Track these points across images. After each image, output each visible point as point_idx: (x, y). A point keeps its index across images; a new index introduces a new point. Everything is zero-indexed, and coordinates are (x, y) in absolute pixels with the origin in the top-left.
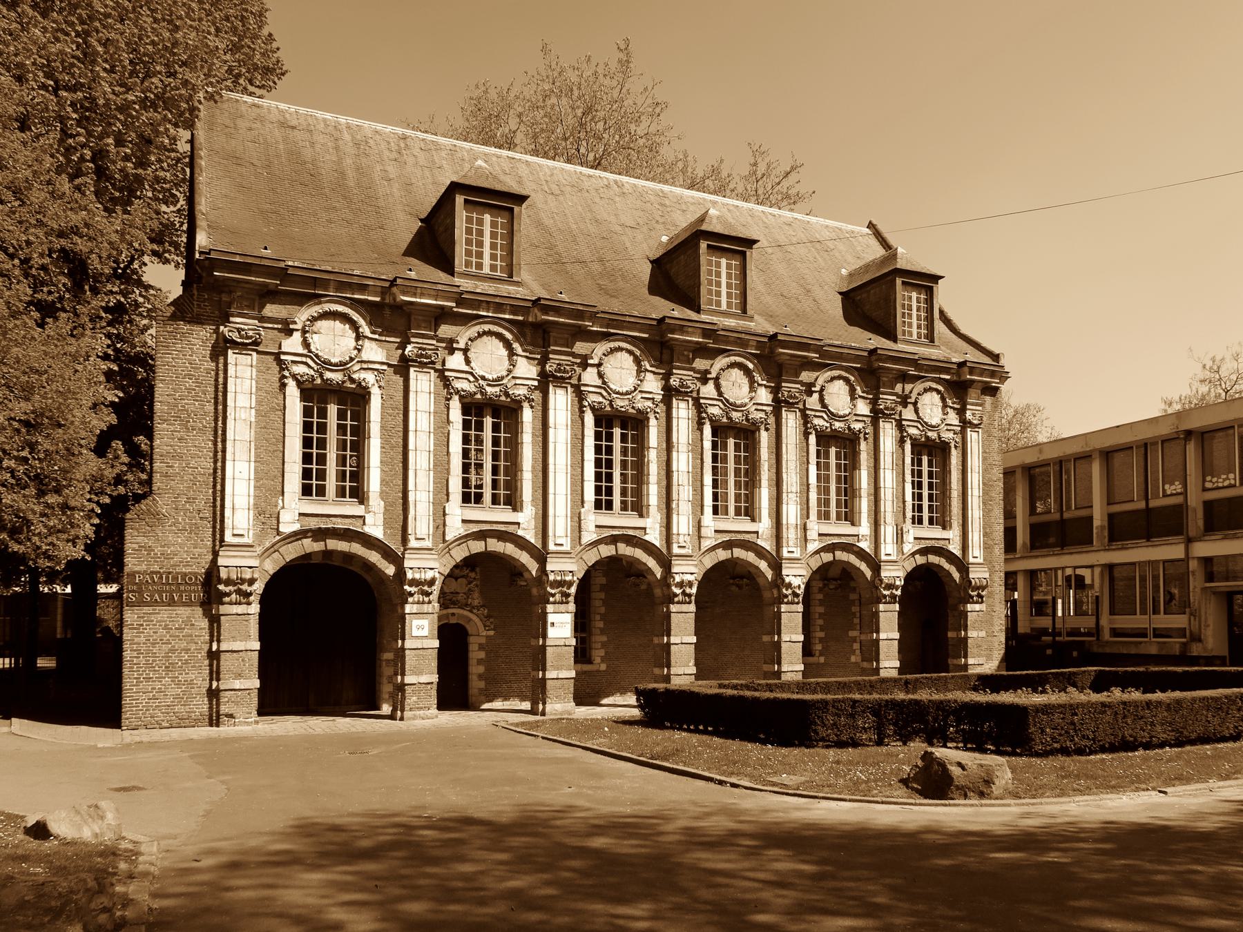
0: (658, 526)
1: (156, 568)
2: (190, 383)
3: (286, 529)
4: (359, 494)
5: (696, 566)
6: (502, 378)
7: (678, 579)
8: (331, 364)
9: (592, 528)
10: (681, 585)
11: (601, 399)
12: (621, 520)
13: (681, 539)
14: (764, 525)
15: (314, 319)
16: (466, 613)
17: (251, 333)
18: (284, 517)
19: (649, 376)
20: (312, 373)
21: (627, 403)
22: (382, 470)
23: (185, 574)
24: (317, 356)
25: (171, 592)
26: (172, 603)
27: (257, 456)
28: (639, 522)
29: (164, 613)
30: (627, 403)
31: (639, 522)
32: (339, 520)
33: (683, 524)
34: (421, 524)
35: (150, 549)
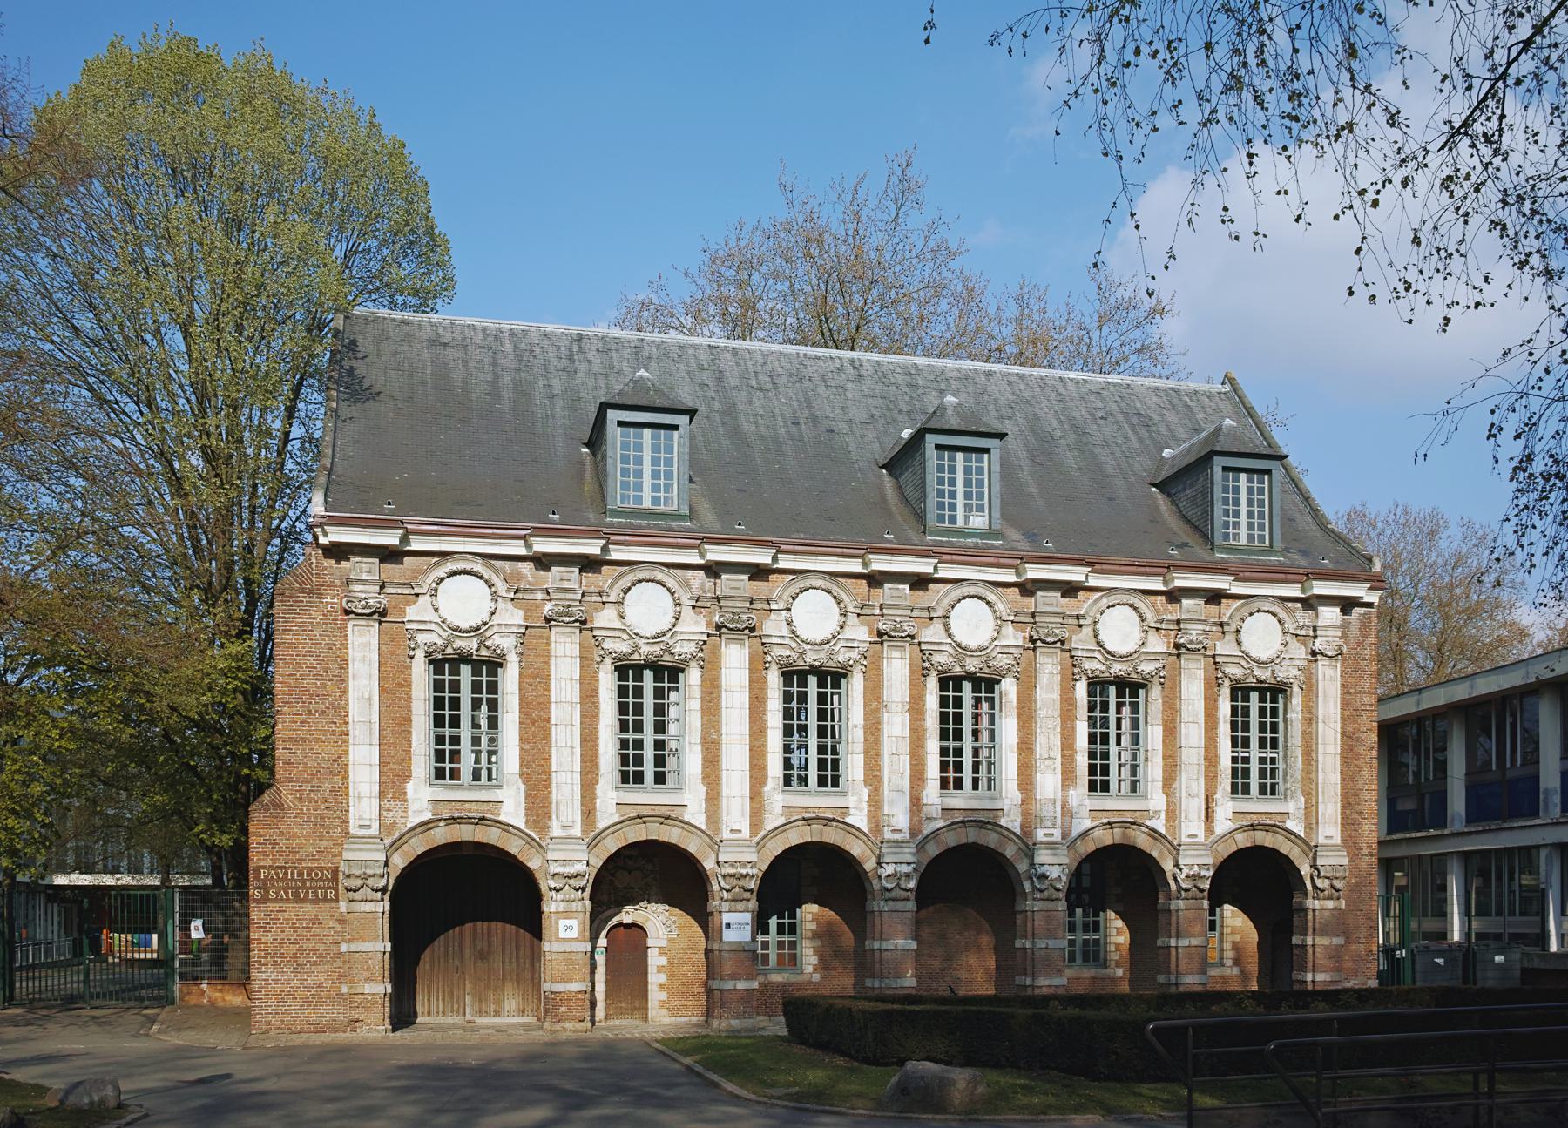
1: (281, 863)
7: (889, 869)
12: (816, 799)
23: (311, 869)
25: (297, 889)
26: (298, 899)
29: (292, 911)
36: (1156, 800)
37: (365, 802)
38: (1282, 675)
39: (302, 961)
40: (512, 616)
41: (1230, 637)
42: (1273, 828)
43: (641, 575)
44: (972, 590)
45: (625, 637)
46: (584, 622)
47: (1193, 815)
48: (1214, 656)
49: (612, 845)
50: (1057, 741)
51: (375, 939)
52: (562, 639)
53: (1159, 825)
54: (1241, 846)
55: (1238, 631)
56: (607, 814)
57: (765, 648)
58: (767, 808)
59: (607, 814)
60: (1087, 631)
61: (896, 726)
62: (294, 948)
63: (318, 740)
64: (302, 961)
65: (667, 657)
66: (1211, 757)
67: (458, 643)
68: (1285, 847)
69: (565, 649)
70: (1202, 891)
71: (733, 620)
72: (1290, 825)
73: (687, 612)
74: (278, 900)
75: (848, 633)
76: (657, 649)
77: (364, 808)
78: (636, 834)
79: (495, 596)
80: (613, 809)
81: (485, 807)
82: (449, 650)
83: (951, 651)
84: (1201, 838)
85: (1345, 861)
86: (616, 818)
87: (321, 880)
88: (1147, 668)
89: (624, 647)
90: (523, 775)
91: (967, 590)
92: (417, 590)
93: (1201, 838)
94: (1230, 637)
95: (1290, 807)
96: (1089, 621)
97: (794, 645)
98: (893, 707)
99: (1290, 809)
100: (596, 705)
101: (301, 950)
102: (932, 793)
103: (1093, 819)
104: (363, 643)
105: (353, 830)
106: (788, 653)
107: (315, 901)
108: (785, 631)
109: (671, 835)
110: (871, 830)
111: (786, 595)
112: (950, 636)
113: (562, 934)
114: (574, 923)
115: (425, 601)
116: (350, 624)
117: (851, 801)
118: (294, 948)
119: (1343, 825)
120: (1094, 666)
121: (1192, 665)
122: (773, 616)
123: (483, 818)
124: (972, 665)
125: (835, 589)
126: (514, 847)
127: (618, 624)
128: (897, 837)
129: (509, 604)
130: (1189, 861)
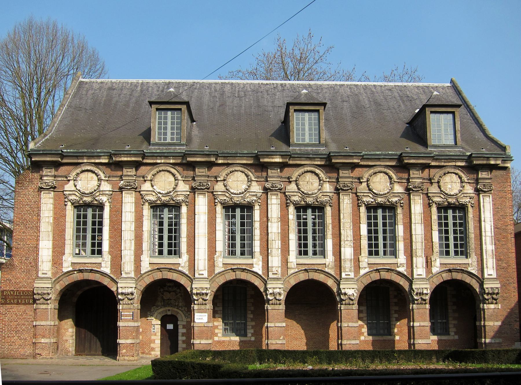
0: (261, 263)
1: (12, 288)
2: (28, 208)
3: (65, 270)
4: (100, 252)
5: (282, 284)
6: (170, 192)
7: (271, 291)
8: (85, 194)
9: (221, 265)
10: (273, 294)
11: (225, 198)
13: (274, 269)
14: (330, 258)
15: (78, 174)
16: (176, 310)
17: (50, 184)
18: (65, 265)
19: (254, 184)
20: (78, 198)
22: (110, 241)
24: (79, 191)
25: (18, 299)
26: (18, 303)
27: (54, 237)
28: (249, 261)
31: (249, 261)
32: (90, 265)
33: (275, 261)
35: (10, 281)
36: (402, 258)
37: (45, 264)
38: (463, 200)
39: (19, 328)
40: (106, 187)
41: (435, 185)
43: (161, 169)
44: (309, 169)
45: (154, 194)
46: (136, 189)
49: (148, 280)
51: (47, 320)
53: (401, 269)
54: (445, 279)
55: (438, 182)
56: (145, 267)
57: (215, 197)
59: (145, 267)
60: (364, 184)
61: (274, 228)
62: (16, 323)
63: (29, 239)
64: (19, 328)
65: (172, 202)
66: (428, 238)
67: (85, 199)
68: (468, 279)
69: (129, 200)
70: (425, 300)
71: (200, 186)
72: (470, 269)
74: (11, 303)
77: (45, 266)
78: (158, 276)
79: (100, 180)
80: (148, 265)
81: (94, 265)
82: (81, 202)
83: (300, 195)
84: (424, 276)
85: (499, 286)
86: (149, 269)
87: (27, 295)
88: (395, 200)
89: (153, 198)
91: (306, 169)
92: (69, 179)
93: (424, 276)
95: (469, 261)
96: (365, 180)
97: (227, 195)
100: (142, 223)
101: (18, 324)
102: (293, 257)
103: (370, 267)
104: (47, 201)
105: (40, 275)
106: (225, 198)
107: (25, 304)
108: (224, 189)
109: (174, 276)
110: (263, 273)
111: (224, 174)
112: (299, 189)
115: (72, 182)
117: (254, 261)
118: (16, 323)
119: (497, 270)
120: (368, 199)
121: (417, 198)
122: (219, 183)
123: (92, 270)
124: (310, 200)
125: (246, 171)
126: (106, 282)
127: (151, 189)
128: (275, 276)
129: (106, 183)
130: (418, 286)
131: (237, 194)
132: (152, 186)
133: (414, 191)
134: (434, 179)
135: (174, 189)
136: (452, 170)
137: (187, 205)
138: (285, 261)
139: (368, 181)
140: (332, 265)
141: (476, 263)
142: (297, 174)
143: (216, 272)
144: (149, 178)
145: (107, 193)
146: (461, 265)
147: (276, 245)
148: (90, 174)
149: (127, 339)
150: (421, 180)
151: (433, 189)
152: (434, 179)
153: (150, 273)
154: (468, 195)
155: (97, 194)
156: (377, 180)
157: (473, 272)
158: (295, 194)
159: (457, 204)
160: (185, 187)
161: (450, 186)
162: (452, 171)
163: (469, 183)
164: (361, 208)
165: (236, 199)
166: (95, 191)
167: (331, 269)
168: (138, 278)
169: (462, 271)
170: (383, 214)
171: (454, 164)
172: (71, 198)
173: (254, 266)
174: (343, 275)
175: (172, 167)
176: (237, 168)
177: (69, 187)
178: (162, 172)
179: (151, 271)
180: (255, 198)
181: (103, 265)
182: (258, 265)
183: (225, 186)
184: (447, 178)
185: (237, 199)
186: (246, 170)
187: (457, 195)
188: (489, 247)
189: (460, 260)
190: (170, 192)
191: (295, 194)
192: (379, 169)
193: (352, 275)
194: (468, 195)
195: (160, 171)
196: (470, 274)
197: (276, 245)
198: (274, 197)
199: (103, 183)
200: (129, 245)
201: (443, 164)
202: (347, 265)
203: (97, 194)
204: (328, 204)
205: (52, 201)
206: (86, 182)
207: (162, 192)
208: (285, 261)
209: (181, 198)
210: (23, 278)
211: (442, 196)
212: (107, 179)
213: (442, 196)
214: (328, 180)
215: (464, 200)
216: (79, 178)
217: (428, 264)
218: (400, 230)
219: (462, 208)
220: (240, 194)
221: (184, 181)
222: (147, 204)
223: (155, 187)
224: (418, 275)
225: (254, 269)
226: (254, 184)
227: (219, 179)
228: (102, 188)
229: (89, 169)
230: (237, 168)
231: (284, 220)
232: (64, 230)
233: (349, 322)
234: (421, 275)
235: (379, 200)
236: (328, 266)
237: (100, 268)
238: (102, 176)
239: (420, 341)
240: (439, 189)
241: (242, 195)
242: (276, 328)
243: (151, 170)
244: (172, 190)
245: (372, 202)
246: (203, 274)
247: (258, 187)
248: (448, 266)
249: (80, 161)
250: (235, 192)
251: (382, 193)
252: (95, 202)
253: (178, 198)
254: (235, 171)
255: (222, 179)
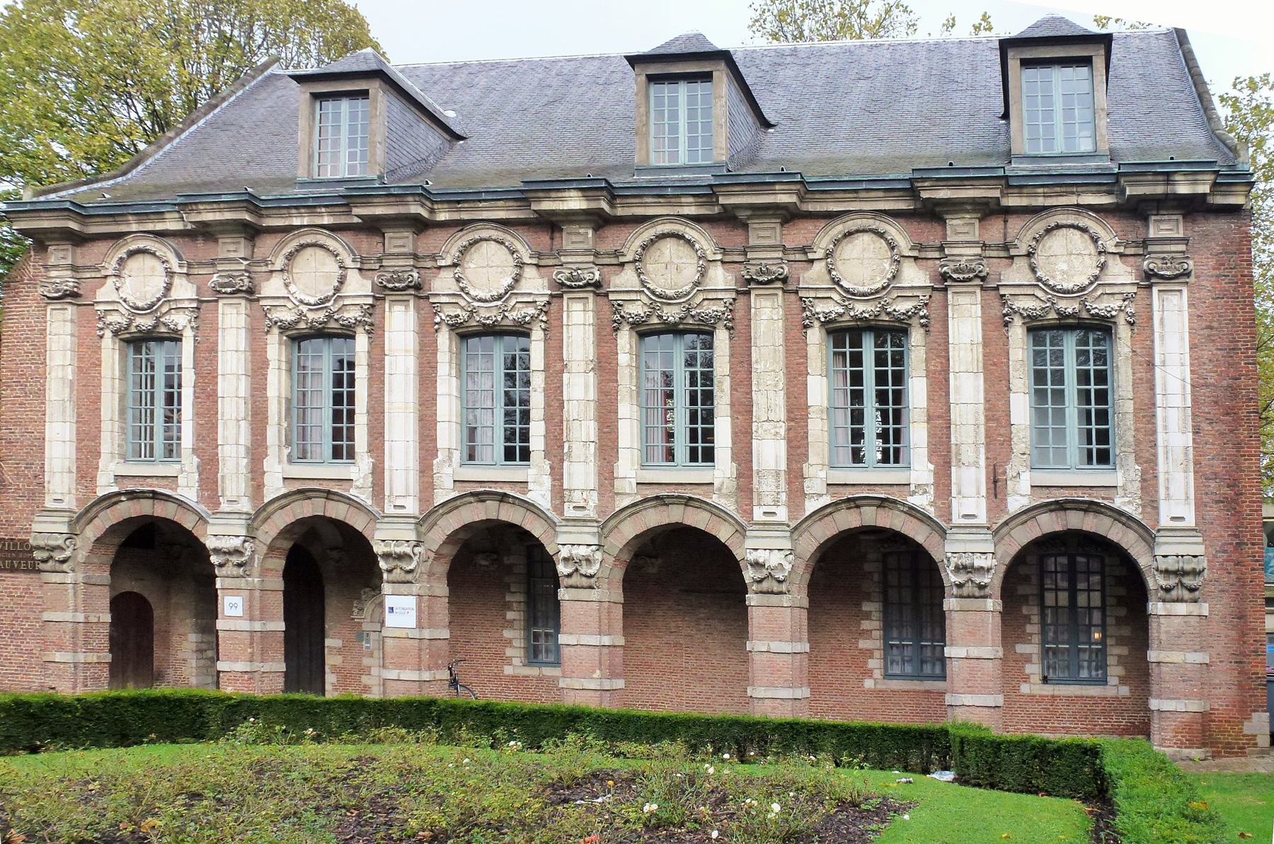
3: (101, 493)
11: (459, 311)
13: (577, 496)
19: (530, 272)
21: (495, 312)
25: (13, 559)
30: (495, 312)
34: (234, 485)
36: (920, 469)
37: (58, 476)
38: (1102, 306)
39: (17, 628)
40: (184, 290)
41: (1021, 264)
42: (1090, 507)
43: (303, 241)
44: (667, 228)
45: (290, 305)
47: (969, 489)
48: (997, 288)
50: (780, 400)
51: (65, 609)
52: (228, 310)
53: (921, 501)
58: (436, 481)
60: (819, 267)
64: (17, 628)
66: (997, 414)
72: (1119, 503)
73: (353, 276)
75: (525, 287)
76: (321, 316)
84: (982, 519)
88: (903, 307)
89: (288, 316)
90: (195, 451)
93: (982, 519)
94: (1021, 264)
95: (1118, 478)
96: (820, 254)
97: (463, 303)
98: (574, 367)
99: (1120, 483)
101: (15, 618)
103: (833, 495)
106: (459, 311)
108: (454, 288)
111: (454, 251)
112: (643, 283)
113: (228, 612)
114: (238, 600)
116: (49, 307)
120: (830, 308)
121: (963, 299)
125: (508, 239)
128: (579, 514)
129: (184, 281)
131: (485, 301)
132: (287, 285)
133: (955, 280)
134: (1016, 247)
135: (337, 290)
136: (1071, 220)
137: (368, 332)
138: (607, 475)
139: (829, 255)
140: (730, 486)
141: (1138, 484)
142: (638, 242)
143: (438, 501)
144: (278, 266)
145: (186, 304)
146: (1094, 492)
147: (582, 430)
148: (148, 261)
149: (236, 660)
150: (978, 251)
151: (1016, 274)
152: (1016, 247)
153: (283, 502)
154: (1116, 290)
155: (165, 309)
156: (855, 255)
157: (1128, 509)
158: (633, 297)
159: (1085, 315)
160: (363, 285)
161: (1064, 267)
162: (1069, 222)
163: (1121, 255)
164: (809, 331)
165: (484, 313)
166: (159, 300)
167: (727, 496)
168: (258, 513)
169: (1090, 507)
170: (872, 344)
171: (1073, 200)
172: (109, 319)
173: (530, 486)
174: (758, 515)
175: (329, 236)
176: (485, 234)
177: (106, 293)
178: (309, 251)
179: (284, 496)
180: (531, 311)
181: (181, 481)
182: (541, 485)
183: (458, 280)
184: (1057, 243)
185: (487, 314)
186: (509, 238)
187: (1083, 289)
188: (1175, 435)
189: (1096, 476)
190: (327, 299)
191: (633, 297)
192: (859, 221)
193: (782, 514)
194: (1116, 290)
195: (303, 247)
196: (1119, 515)
197: (582, 430)
198: (577, 306)
199: (177, 281)
200: (234, 431)
201: (1040, 201)
202: (769, 488)
203: (165, 309)
204: (720, 325)
205: (69, 328)
206: (139, 281)
207: (307, 299)
208: (607, 475)
209: (352, 314)
210: (22, 511)
211: (1040, 294)
212: (185, 270)
213: (1040, 294)
214: (719, 257)
215: (1102, 306)
216: (125, 272)
217: (996, 485)
218: (917, 390)
219: (1099, 328)
220: (494, 299)
221: (360, 269)
222: (276, 331)
223: (292, 288)
224: (965, 516)
225: (529, 497)
226: (530, 272)
227: (442, 263)
228: (174, 294)
229: (141, 246)
230: (485, 234)
231: (605, 366)
232: (98, 399)
233: (773, 639)
234: (973, 516)
235: (860, 308)
236: (720, 489)
237: (175, 489)
238: (174, 263)
239: (967, 699)
240: (1031, 275)
241: (499, 303)
242: (584, 648)
243: (282, 244)
244: (331, 294)
245: (841, 315)
246: (403, 507)
247: (540, 281)
248: (1054, 491)
249: (124, 228)
250: (482, 295)
251: (865, 289)
252: (163, 329)
253: (346, 315)
254: (482, 240)
255: (449, 263)
